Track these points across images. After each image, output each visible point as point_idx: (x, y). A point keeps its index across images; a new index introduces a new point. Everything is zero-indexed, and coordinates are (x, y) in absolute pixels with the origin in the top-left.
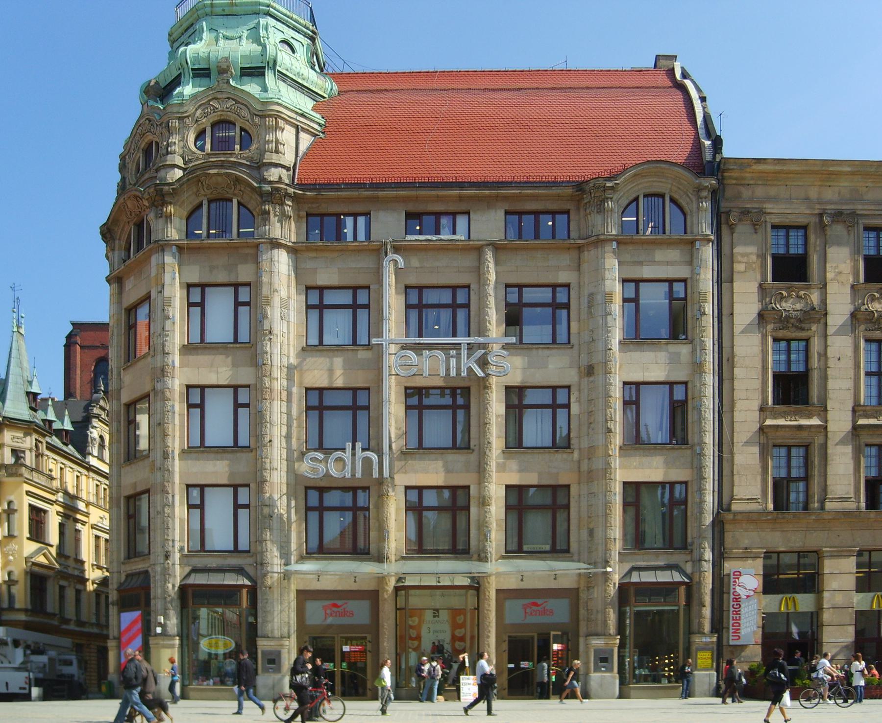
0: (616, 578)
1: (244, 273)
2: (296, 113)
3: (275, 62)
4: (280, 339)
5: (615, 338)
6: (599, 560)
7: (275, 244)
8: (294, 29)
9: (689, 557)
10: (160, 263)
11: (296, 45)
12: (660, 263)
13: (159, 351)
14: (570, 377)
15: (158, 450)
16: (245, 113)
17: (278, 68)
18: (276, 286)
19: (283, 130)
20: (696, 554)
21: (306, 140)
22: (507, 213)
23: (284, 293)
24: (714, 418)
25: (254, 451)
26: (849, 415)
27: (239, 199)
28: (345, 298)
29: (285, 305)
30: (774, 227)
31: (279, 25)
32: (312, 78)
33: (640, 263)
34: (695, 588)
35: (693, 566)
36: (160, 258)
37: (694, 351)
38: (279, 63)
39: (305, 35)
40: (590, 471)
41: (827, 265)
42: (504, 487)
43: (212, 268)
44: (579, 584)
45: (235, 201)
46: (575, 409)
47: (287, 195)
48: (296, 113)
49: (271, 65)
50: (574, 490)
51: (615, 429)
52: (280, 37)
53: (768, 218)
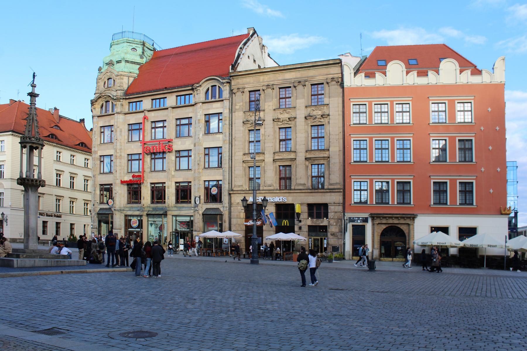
12: (214, 108)
14: (191, 147)
19: (123, 79)
21: (131, 80)
22: (177, 96)
24: (229, 159)
26: (272, 155)
29: (121, 131)
31: (131, 44)
33: (209, 109)
38: (125, 58)
43: (105, 122)
48: (128, 72)
49: (123, 59)
53: (246, 89)
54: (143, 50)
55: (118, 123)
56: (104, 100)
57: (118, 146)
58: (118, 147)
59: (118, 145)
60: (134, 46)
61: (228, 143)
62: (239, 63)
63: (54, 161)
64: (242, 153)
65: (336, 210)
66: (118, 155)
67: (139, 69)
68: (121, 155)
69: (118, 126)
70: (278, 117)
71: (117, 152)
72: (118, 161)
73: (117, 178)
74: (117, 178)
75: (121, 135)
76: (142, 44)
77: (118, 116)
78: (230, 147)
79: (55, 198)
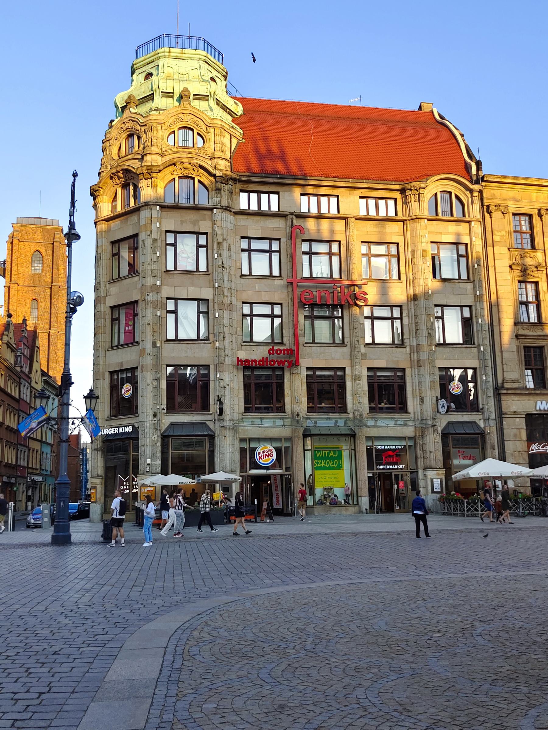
0: (440, 430)
1: (204, 226)
6: (429, 418)
9: (481, 417)
10: (149, 216)
13: (149, 275)
15: (149, 341)
17: (216, 97)
19: (224, 136)
20: (486, 416)
25: (212, 343)
27: (199, 178)
28: (264, 245)
30: (514, 214)
32: (231, 104)
34: (487, 437)
35: (485, 423)
36: (149, 213)
40: (419, 361)
43: (182, 222)
44: (416, 433)
46: (406, 320)
49: (212, 94)
50: (408, 372)
52: (210, 75)
55: (224, 229)
56: (180, 172)
57: (225, 282)
58: (226, 284)
59: (226, 278)
66: (227, 301)
69: (225, 237)
71: (226, 294)
73: (227, 352)
74: (227, 352)
75: (230, 257)
77: (224, 214)
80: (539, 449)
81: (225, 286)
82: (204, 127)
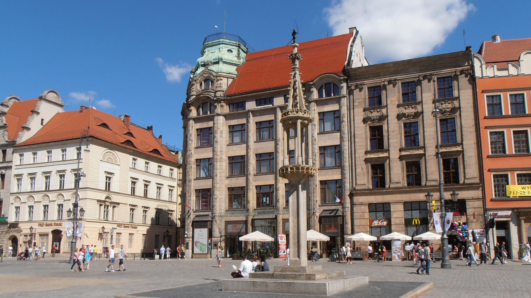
2: (227, 73)
3: (222, 59)
4: (220, 143)
5: (315, 133)
7: (218, 115)
8: (232, 45)
11: (232, 50)
16: (212, 76)
18: (218, 127)
19: (222, 80)
21: (230, 81)
23: (221, 129)
24: (349, 157)
29: (221, 132)
31: (227, 46)
37: (341, 135)
39: (236, 46)
41: (388, 99)
42: (284, 184)
45: (209, 103)
47: (222, 100)
48: (227, 73)
51: (316, 163)
54: (239, 51)
60: (230, 47)
61: (347, 141)
62: (352, 60)
63: (130, 168)
64: (363, 151)
65: (476, 206)
67: (237, 70)
68: (221, 158)
70: (403, 112)
72: (219, 164)
76: (238, 45)
78: (350, 145)
79: (129, 207)
80: (379, 224)
81: (218, 151)
82: (213, 78)
